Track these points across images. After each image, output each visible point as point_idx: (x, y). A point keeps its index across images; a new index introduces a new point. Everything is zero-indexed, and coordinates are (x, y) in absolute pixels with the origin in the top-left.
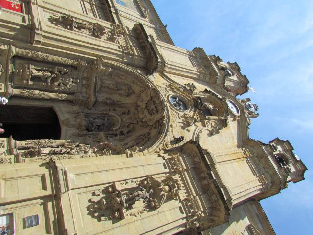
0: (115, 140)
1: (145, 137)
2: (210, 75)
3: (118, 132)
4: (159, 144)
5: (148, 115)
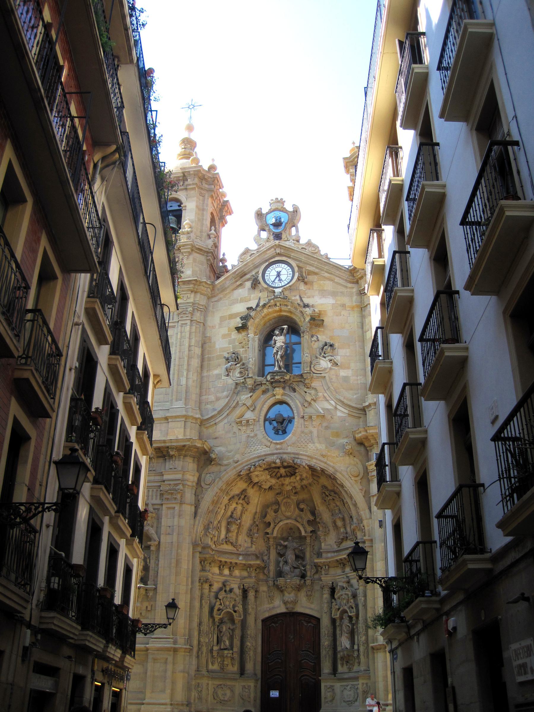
0: (325, 540)
2: (196, 292)
3: (310, 529)
5: (292, 479)
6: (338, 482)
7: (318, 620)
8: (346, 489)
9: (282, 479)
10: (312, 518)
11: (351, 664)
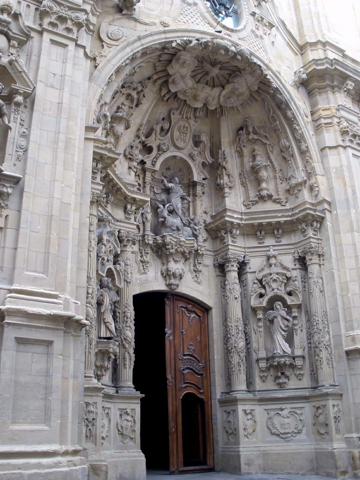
1: (255, 133)
4: (305, 129)
5: (216, 91)
6: (289, 114)
7: (206, 309)
8: (297, 128)
9: (200, 86)
10: (210, 160)
11: (287, 377)
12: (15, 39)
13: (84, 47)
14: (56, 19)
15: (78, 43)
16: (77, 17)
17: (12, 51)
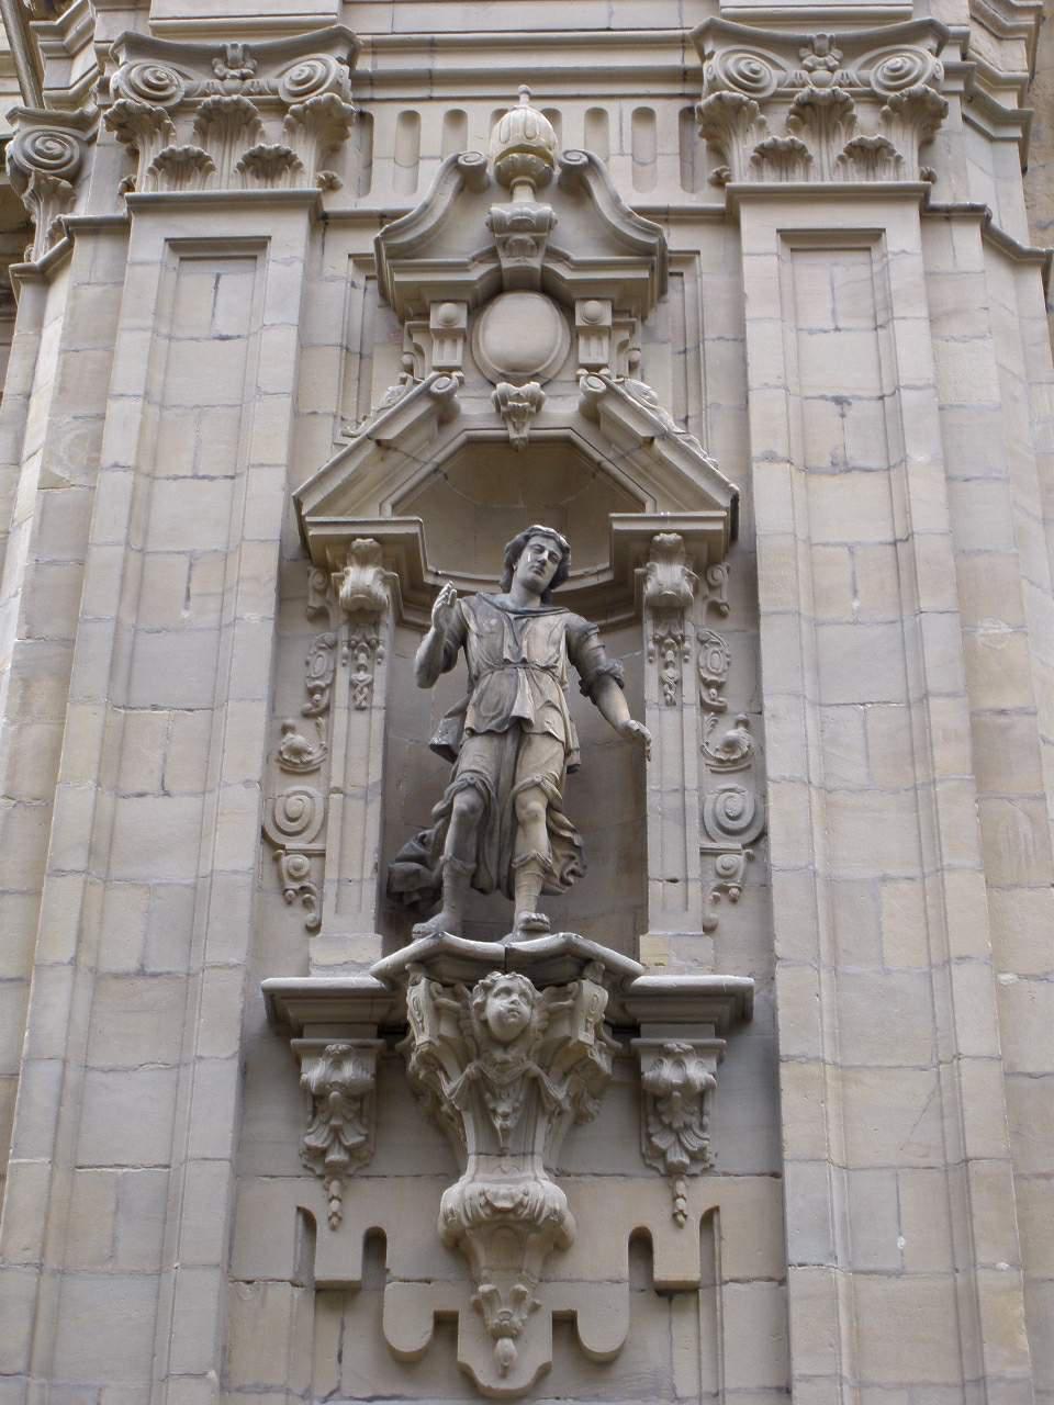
12: (593, 290)
13: (975, 214)
14: (793, 126)
15: (941, 197)
16: (897, 74)
17: (593, 351)
